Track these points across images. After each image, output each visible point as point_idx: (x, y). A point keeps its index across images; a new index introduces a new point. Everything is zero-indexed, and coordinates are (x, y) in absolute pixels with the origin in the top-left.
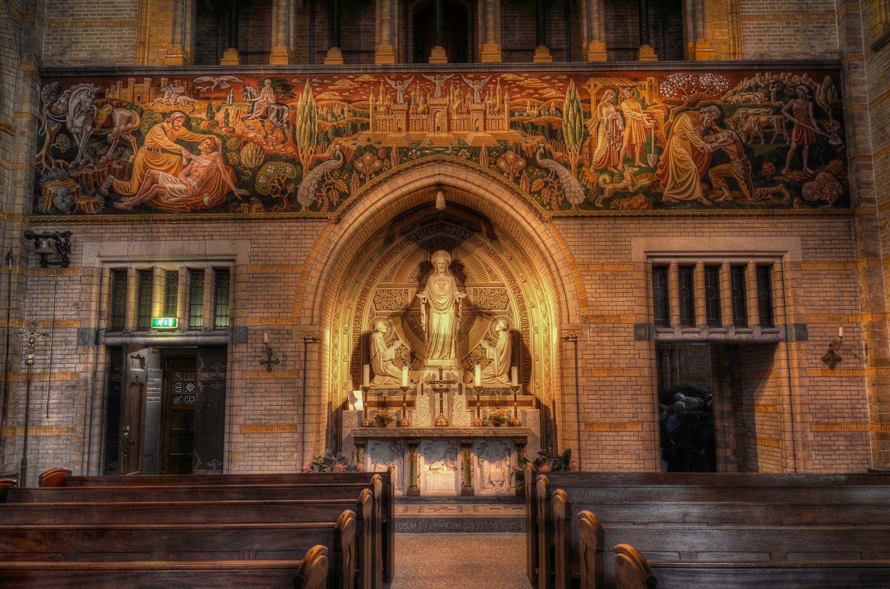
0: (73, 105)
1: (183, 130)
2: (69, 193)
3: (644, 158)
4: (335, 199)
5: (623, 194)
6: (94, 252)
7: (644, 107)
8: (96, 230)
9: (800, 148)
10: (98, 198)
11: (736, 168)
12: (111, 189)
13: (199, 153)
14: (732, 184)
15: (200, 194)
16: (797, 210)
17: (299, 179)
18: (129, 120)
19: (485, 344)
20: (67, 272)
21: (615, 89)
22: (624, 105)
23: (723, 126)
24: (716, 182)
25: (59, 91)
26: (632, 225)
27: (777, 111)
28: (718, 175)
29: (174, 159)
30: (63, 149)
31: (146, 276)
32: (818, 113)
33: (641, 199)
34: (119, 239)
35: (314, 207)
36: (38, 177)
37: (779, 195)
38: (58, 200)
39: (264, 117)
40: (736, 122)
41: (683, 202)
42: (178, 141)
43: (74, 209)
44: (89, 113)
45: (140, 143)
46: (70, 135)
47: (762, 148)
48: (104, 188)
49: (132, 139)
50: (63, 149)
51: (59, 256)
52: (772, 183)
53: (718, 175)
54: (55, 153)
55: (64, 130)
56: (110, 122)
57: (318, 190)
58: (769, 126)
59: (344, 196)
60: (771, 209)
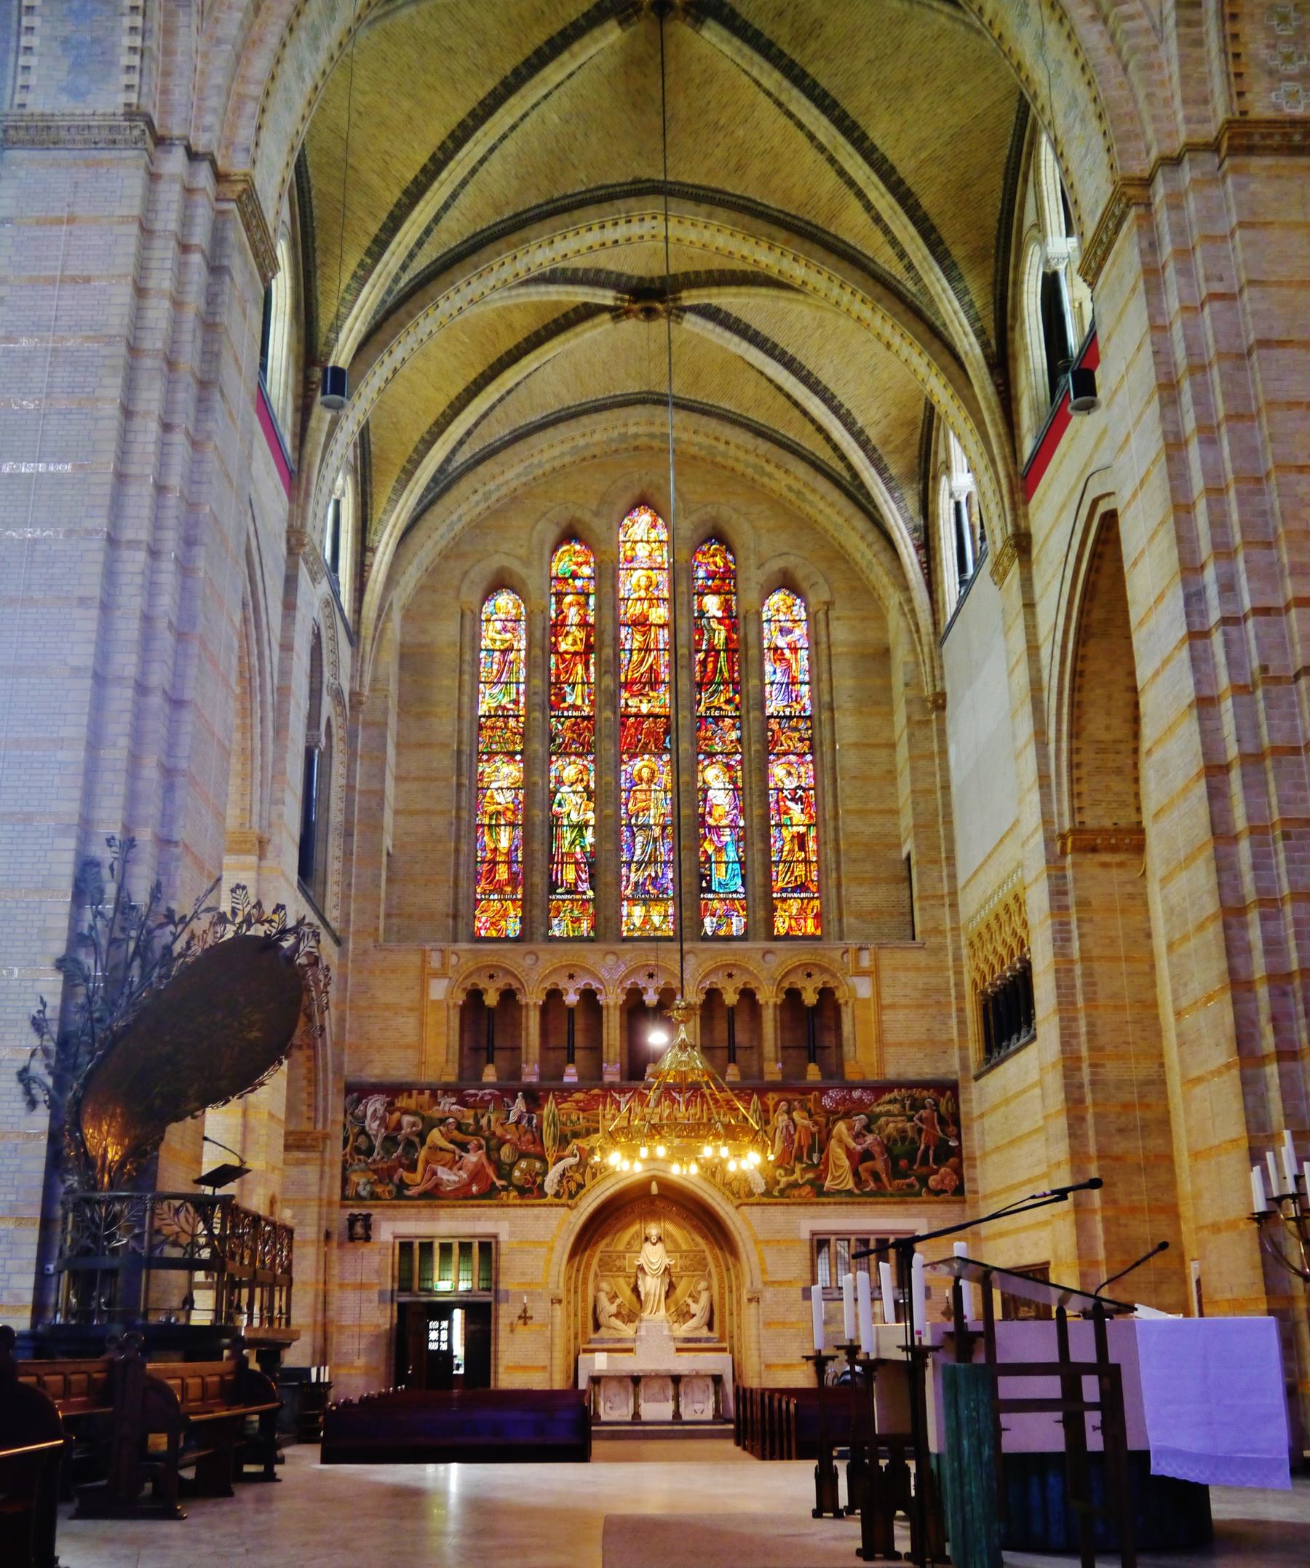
0: (369, 1112)
1: (456, 1133)
2: (368, 1182)
3: (810, 1158)
4: (573, 1187)
5: (794, 1185)
6: (392, 1227)
7: (810, 1116)
8: (390, 1212)
9: (927, 1148)
10: (391, 1187)
11: (879, 1165)
12: (401, 1179)
13: (467, 1151)
14: (876, 1176)
15: (470, 1184)
16: (924, 1196)
17: (545, 1173)
18: (414, 1124)
19: (689, 1301)
20: (368, 1245)
21: (789, 1102)
22: (795, 1115)
23: (871, 1132)
24: (864, 1176)
25: (359, 1101)
26: (802, 1210)
27: (910, 1119)
28: (866, 1170)
29: (449, 1156)
30: (364, 1147)
31: (427, 1248)
32: (942, 1121)
33: (808, 1189)
34: (407, 1219)
35: (557, 1195)
36: (344, 1169)
37: (911, 1186)
38: (360, 1188)
39: (518, 1122)
40: (880, 1128)
41: (839, 1192)
42: (452, 1142)
43: (374, 1196)
44: (383, 1119)
45: (423, 1142)
46: (368, 1136)
47: (899, 1148)
48: (396, 1179)
49: (417, 1140)
50: (364, 1147)
51: (359, 1230)
52: (906, 1176)
53: (866, 1170)
54: (357, 1150)
55: (363, 1131)
56: (399, 1126)
57: (560, 1182)
58: (904, 1131)
59: (581, 1186)
60: (905, 1196)
